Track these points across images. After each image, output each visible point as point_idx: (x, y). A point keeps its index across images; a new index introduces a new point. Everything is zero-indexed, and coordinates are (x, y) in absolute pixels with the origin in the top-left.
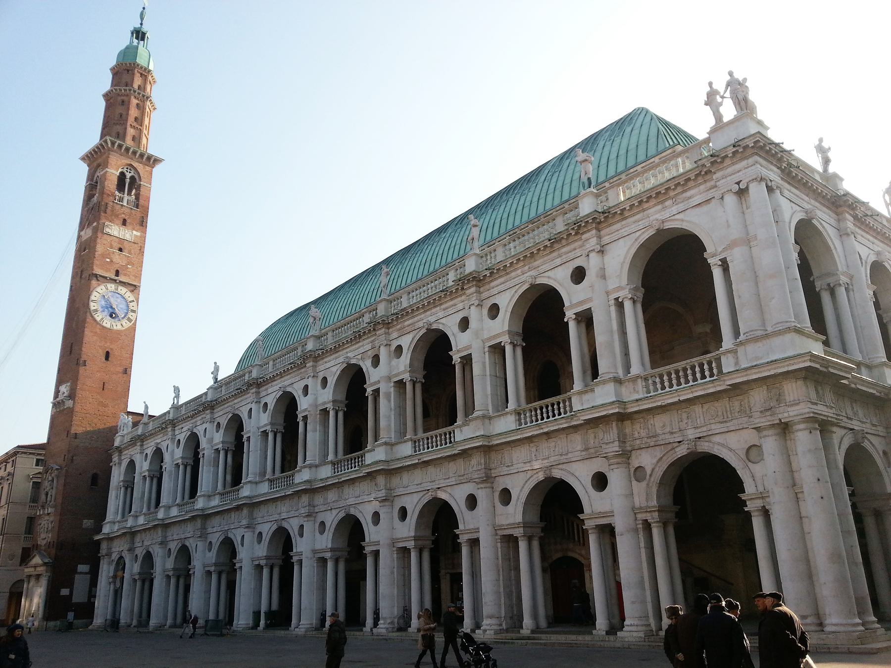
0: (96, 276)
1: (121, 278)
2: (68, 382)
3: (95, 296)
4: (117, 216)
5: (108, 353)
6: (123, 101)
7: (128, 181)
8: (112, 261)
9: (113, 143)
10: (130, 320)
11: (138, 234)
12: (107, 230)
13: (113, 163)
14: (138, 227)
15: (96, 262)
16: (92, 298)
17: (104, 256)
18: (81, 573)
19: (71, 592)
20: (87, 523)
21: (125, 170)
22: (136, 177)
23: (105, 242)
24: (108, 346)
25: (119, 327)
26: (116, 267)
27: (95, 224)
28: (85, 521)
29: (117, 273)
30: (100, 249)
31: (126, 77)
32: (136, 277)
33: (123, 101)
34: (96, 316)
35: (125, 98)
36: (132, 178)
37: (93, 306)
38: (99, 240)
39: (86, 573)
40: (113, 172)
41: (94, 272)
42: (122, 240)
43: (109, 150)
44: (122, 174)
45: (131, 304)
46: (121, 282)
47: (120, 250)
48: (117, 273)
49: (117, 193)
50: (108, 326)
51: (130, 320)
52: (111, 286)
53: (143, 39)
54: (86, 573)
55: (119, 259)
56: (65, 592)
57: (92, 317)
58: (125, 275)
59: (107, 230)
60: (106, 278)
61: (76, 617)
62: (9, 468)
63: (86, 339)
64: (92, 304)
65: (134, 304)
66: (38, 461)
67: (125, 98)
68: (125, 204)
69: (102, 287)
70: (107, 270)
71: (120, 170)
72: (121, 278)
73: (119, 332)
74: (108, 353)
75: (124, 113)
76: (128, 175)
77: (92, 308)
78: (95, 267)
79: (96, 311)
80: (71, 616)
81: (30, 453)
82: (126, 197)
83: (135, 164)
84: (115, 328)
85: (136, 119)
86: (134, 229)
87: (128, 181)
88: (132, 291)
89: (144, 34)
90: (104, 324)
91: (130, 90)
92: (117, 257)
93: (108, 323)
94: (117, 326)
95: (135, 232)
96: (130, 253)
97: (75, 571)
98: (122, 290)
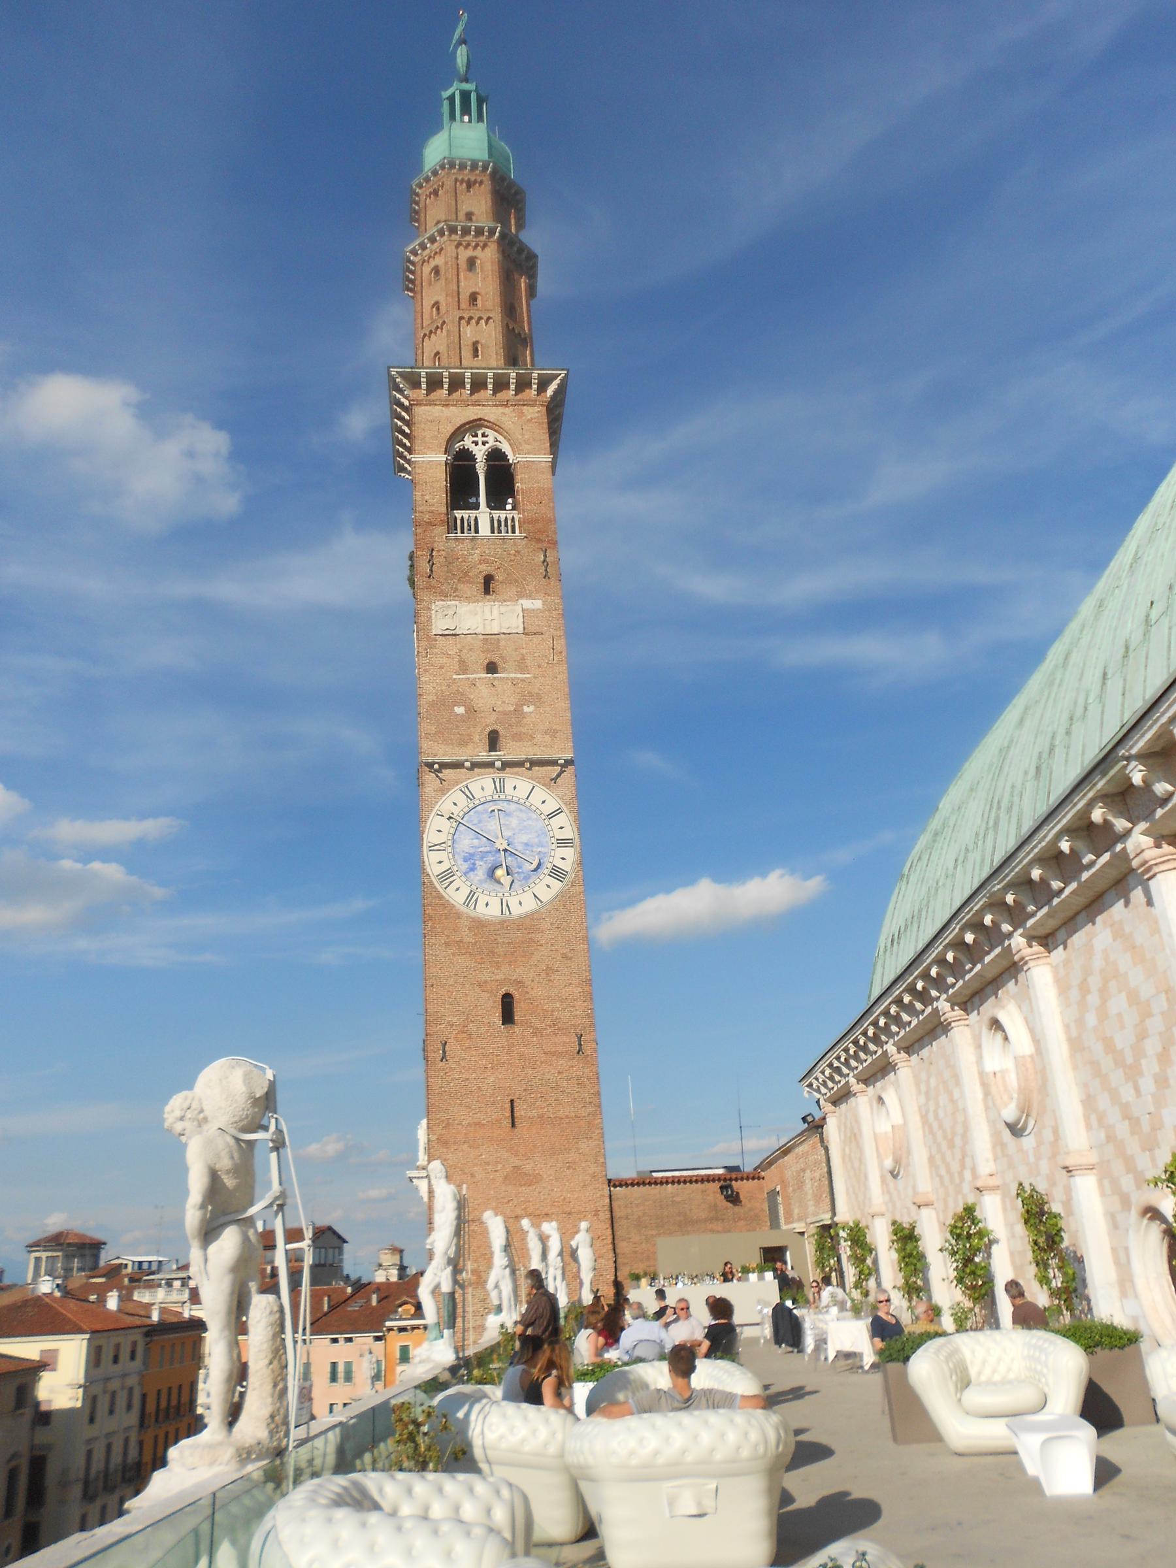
0: (430, 765)
3: (435, 830)
4: (465, 577)
6: (436, 271)
8: (472, 711)
10: (557, 873)
11: (538, 604)
12: (439, 625)
13: (428, 434)
15: (427, 727)
17: (443, 703)
21: (467, 442)
22: (505, 447)
24: (502, 976)
25: (530, 905)
26: (490, 722)
29: (494, 741)
30: (430, 687)
32: (553, 733)
33: (436, 271)
35: (439, 261)
36: (496, 456)
37: (435, 863)
41: (425, 759)
42: (490, 640)
46: (506, 765)
47: (492, 668)
49: (458, 514)
51: (557, 873)
52: (482, 785)
55: (491, 697)
57: (441, 897)
58: (518, 738)
59: (439, 625)
60: (457, 765)
68: (484, 529)
69: (456, 795)
70: (464, 741)
73: (531, 922)
75: (441, 299)
76: (480, 453)
78: (425, 745)
79: (447, 875)
82: (484, 515)
83: (490, 413)
84: (517, 911)
85: (473, 297)
86: (521, 595)
90: (481, 909)
92: (484, 690)
93: (489, 908)
94: (523, 904)
95: (527, 603)
96: (522, 666)
98: (518, 785)
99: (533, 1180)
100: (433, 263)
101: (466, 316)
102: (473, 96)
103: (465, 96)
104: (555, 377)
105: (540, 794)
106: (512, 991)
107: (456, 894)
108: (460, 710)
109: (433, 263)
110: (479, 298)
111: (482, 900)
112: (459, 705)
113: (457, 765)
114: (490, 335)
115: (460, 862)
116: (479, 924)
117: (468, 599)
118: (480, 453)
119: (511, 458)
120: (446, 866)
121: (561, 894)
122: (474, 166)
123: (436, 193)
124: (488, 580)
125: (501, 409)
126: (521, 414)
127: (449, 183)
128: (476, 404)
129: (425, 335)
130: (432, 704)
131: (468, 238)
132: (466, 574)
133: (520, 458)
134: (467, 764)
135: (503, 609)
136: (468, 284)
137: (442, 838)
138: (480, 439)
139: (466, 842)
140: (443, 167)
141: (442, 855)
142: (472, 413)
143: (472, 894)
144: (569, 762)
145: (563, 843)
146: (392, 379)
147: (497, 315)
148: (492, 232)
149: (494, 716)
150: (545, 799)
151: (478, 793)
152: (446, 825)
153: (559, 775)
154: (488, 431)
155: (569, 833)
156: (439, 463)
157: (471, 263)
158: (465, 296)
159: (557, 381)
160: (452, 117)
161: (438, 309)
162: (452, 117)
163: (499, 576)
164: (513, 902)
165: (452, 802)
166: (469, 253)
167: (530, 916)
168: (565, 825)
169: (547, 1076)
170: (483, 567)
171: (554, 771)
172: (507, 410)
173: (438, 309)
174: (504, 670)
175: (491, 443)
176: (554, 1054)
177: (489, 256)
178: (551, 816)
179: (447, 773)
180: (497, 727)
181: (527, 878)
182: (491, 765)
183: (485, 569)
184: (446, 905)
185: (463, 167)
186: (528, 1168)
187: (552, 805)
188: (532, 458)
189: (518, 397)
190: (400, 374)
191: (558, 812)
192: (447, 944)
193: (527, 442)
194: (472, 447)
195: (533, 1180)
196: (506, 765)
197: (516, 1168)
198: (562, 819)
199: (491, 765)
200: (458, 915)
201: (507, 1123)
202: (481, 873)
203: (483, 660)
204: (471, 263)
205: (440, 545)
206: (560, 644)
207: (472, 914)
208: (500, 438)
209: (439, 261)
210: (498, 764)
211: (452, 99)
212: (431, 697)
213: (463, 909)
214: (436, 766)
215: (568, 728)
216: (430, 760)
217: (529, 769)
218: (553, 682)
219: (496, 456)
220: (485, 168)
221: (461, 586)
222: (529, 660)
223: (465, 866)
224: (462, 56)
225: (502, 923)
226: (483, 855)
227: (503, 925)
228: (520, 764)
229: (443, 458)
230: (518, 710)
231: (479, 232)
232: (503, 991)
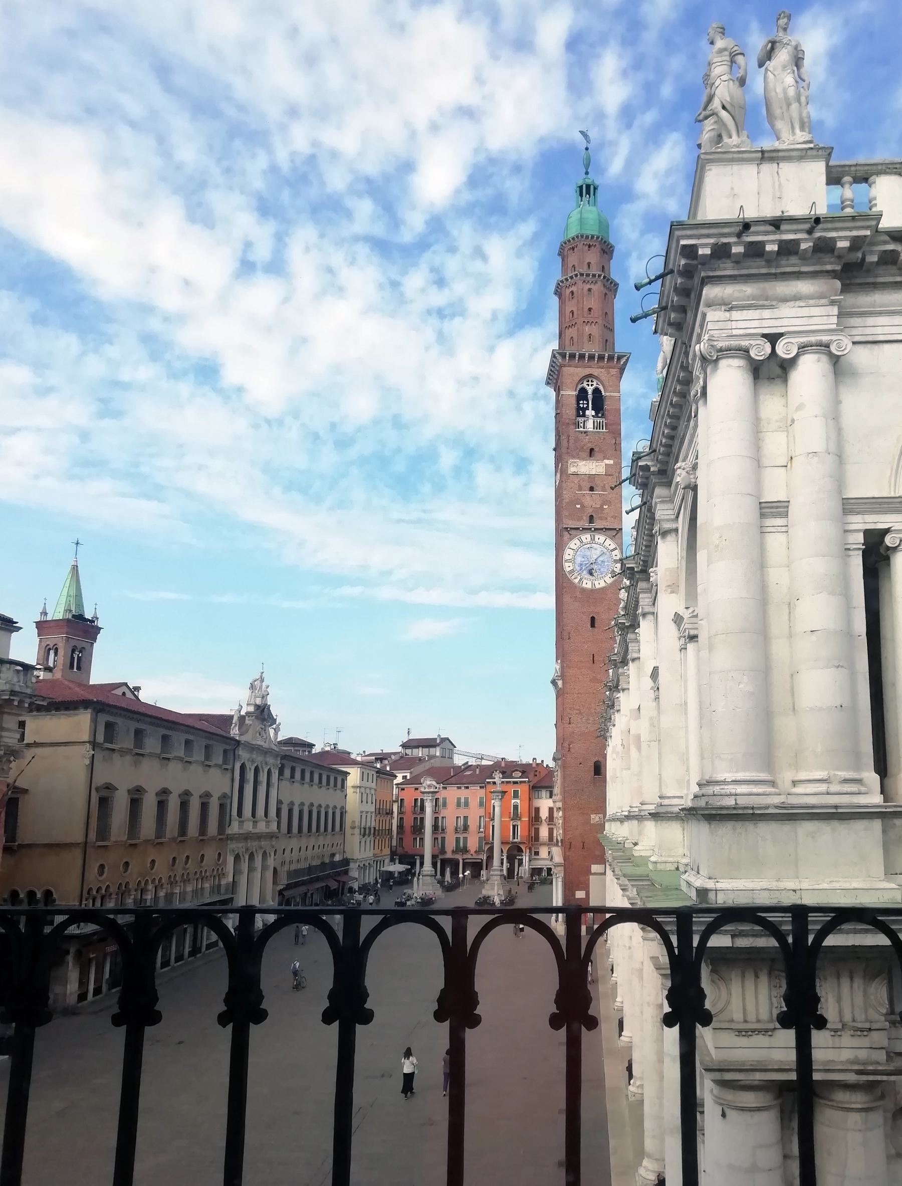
1: (598, 524)
3: (568, 554)
4: (582, 449)
5: (593, 619)
6: (572, 293)
7: (590, 397)
8: (583, 506)
9: (563, 356)
11: (611, 462)
16: (566, 557)
17: (573, 503)
18: (595, 874)
19: (588, 894)
22: (601, 388)
25: (603, 584)
26: (590, 511)
28: (593, 816)
29: (591, 519)
30: (567, 495)
31: (573, 259)
32: (615, 517)
33: (572, 293)
35: (573, 288)
36: (596, 391)
40: (571, 393)
42: (591, 477)
43: (561, 366)
45: (614, 553)
47: (592, 489)
48: (591, 517)
50: (589, 586)
52: (586, 537)
53: (588, 192)
55: (591, 501)
56: (580, 894)
58: (601, 518)
59: (572, 470)
65: (617, 552)
69: (576, 541)
71: (580, 386)
72: (598, 524)
74: (593, 619)
76: (590, 390)
77: (568, 569)
79: (572, 571)
83: (595, 372)
84: (598, 586)
85: (590, 309)
86: (605, 458)
87: (590, 397)
88: (613, 538)
90: (584, 585)
91: (576, 275)
92: (588, 498)
93: (587, 584)
95: (607, 462)
96: (604, 489)
97: (589, 872)
98: (600, 538)
100: (571, 289)
102: (592, 188)
103: (588, 186)
105: (608, 541)
108: (578, 506)
109: (571, 289)
114: (595, 330)
116: (584, 590)
117: (584, 459)
118: (590, 390)
120: (571, 568)
122: (593, 237)
123: (573, 249)
124: (592, 450)
126: (609, 373)
131: (588, 279)
133: (607, 394)
137: (570, 557)
138: (590, 383)
139: (579, 559)
140: (577, 237)
141: (570, 564)
142: (588, 371)
143: (581, 579)
147: (600, 321)
148: (599, 276)
149: (591, 510)
151: (584, 541)
152: (571, 552)
158: (586, 309)
160: (581, 195)
162: (581, 195)
163: (596, 449)
164: (596, 583)
165: (574, 544)
166: (588, 286)
167: (602, 589)
171: (614, 533)
177: (597, 288)
178: (612, 550)
179: (573, 532)
183: (590, 445)
185: (587, 237)
187: (613, 546)
188: (612, 394)
191: (615, 549)
200: (576, 587)
204: (590, 290)
205: (572, 434)
209: (573, 288)
211: (581, 187)
219: (596, 391)
227: (593, 591)
229: (575, 393)
230: (602, 507)
231: (594, 276)
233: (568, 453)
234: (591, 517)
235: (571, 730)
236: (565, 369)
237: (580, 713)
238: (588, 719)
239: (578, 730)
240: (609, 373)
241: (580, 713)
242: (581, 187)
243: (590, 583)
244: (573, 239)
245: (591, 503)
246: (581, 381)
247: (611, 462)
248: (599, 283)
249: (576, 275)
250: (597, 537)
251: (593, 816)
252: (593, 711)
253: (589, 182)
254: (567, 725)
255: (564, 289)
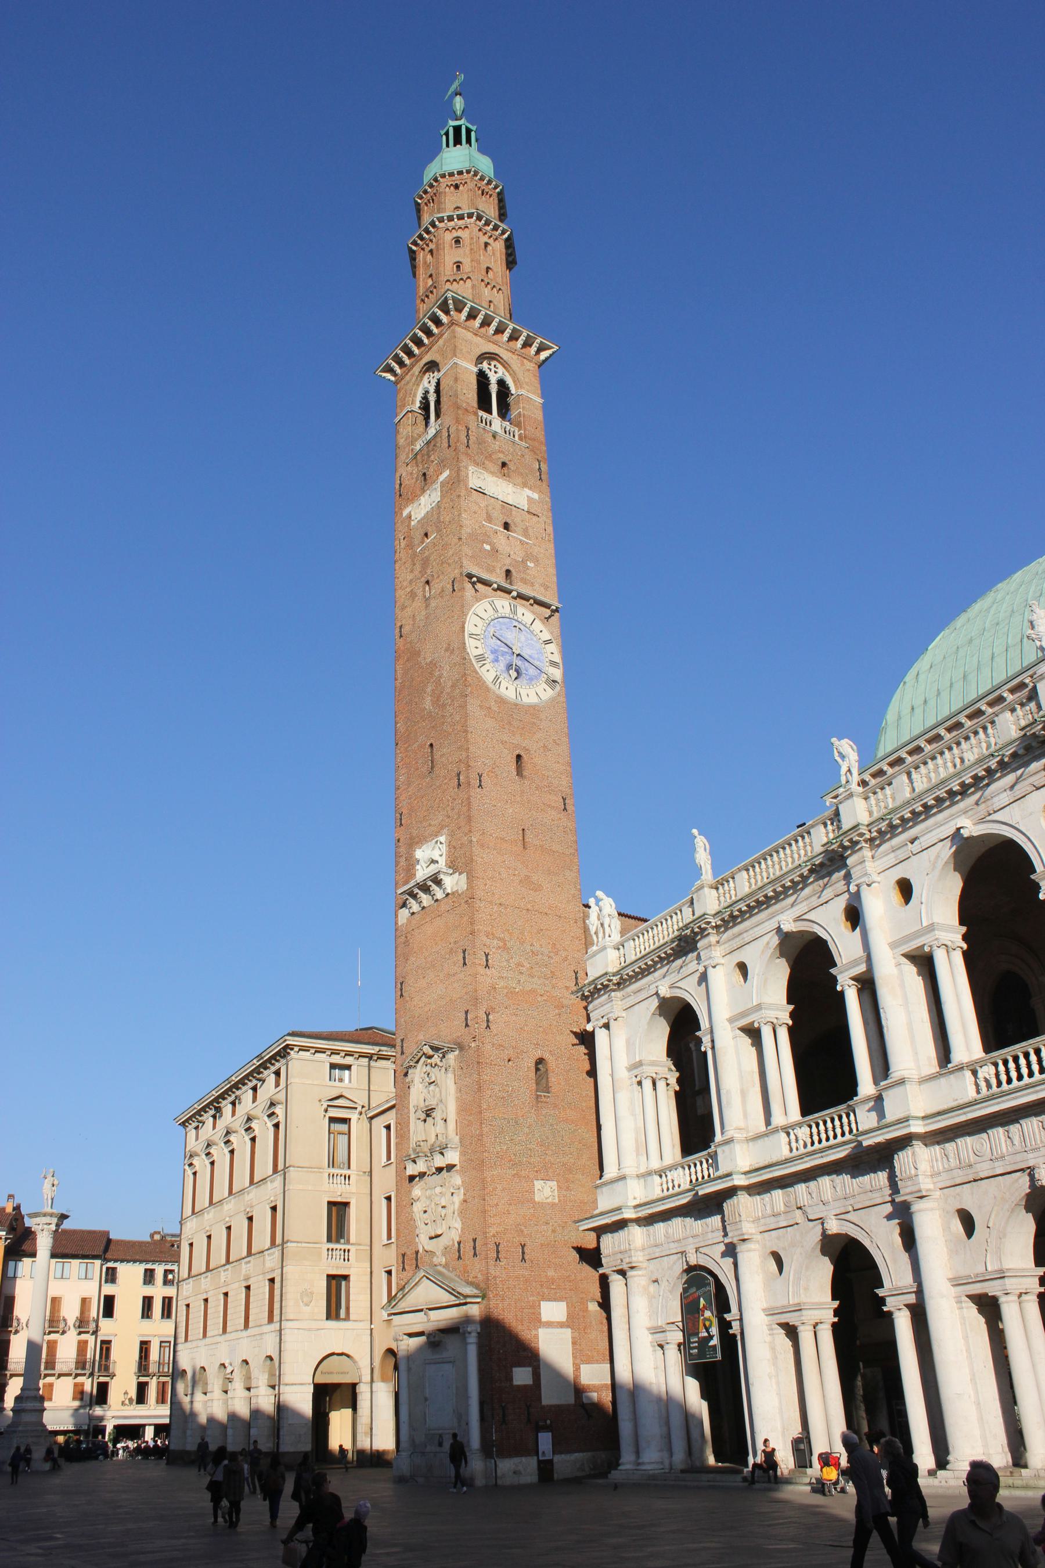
0: (470, 576)
2: (437, 834)
4: (489, 457)
5: (519, 757)
6: (457, 241)
7: (494, 389)
8: (495, 551)
11: (536, 496)
12: (474, 482)
14: (533, 480)
15: (467, 550)
16: (469, 628)
18: (549, 1324)
19: (536, 1376)
20: (545, 1191)
21: (485, 365)
23: (475, 508)
25: (533, 700)
26: (507, 563)
27: (446, 474)
28: (538, 1184)
30: (469, 523)
32: (546, 588)
33: (457, 241)
34: (482, 671)
35: (460, 233)
36: (501, 383)
38: (464, 504)
39: (561, 1325)
43: (452, 323)
44: (482, 379)
46: (521, 596)
47: (506, 526)
49: (481, 413)
52: (503, 604)
53: (469, 141)
54: (561, 1325)
55: (510, 547)
56: (522, 1376)
57: (477, 673)
58: (524, 581)
59: (474, 482)
60: (487, 583)
61: (558, 1446)
62: (268, 1089)
63: (471, 722)
64: (471, 644)
66: (333, 1066)
67: (460, 233)
70: (491, 570)
72: (519, 587)
76: (493, 379)
79: (481, 658)
80: (545, 1440)
81: (319, 1051)
84: (526, 700)
85: (488, 269)
86: (525, 485)
87: (494, 389)
89: (469, 131)
93: (508, 689)
95: (527, 492)
96: (526, 532)
97: (537, 1321)
98: (526, 614)
99: (538, 888)
100: (455, 234)
101: (486, 281)
102: (473, 134)
103: (469, 131)
104: (550, 348)
105: (538, 625)
106: (522, 754)
107: (488, 673)
108: (488, 547)
109: (455, 234)
110: (490, 272)
111: (504, 684)
112: (487, 543)
113: (487, 583)
115: (489, 652)
116: (501, 701)
117: (492, 473)
119: (513, 391)
121: (553, 700)
123: (457, 187)
125: (510, 354)
126: (523, 364)
127: (471, 185)
128: (495, 343)
129: (448, 281)
130: (470, 535)
132: (490, 455)
134: (495, 586)
135: (514, 490)
136: (485, 261)
138: (492, 367)
140: (468, 172)
141: (478, 644)
142: (491, 348)
143: (497, 678)
144: (557, 610)
145: (553, 664)
146: (446, 300)
149: (508, 561)
150: (543, 631)
153: (550, 617)
154: (498, 365)
155: (557, 658)
156: (472, 372)
157: (486, 244)
159: (550, 352)
161: (458, 267)
163: (511, 466)
164: (523, 692)
166: (485, 239)
167: (533, 707)
168: (553, 653)
169: (545, 820)
170: (501, 455)
171: (547, 612)
172: (515, 357)
173: (458, 267)
174: (515, 532)
175: (500, 375)
176: (549, 806)
178: (548, 642)
179: (479, 586)
180: (511, 569)
181: (531, 679)
182: (509, 592)
184: (480, 679)
186: (535, 878)
187: (546, 636)
188: (531, 396)
189: (523, 351)
190: (454, 298)
192: (481, 707)
193: (527, 384)
194: (488, 372)
195: (538, 888)
196: (521, 596)
197: (527, 877)
198: (552, 647)
199: (509, 592)
200: (488, 689)
201: (520, 844)
202: (502, 665)
203: (502, 519)
206: (550, 529)
207: (497, 692)
208: (506, 374)
210: (514, 594)
212: (469, 530)
213: (491, 686)
214: (474, 579)
215: (554, 587)
216: (474, 572)
217: (532, 605)
218: (546, 551)
219: (501, 383)
220: (496, 188)
221: (487, 462)
222: (530, 531)
223: (492, 657)
224: (459, 103)
225: (516, 705)
226: (504, 654)
228: (526, 598)
229: (475, 370)
232: (517, 752)
233: (467, 454)
234: (508, 573)
235: (489, 980)
236: (458, 329)
237: (505, 948)
238: (519, 964)
239: (502, 984)
240: (523, 364)
241: (505, 948)
242: (457, 130)
243: (512, 689)
244: (460, 173)
245: (508, 549)
246: (482, 358)
247: (536, 496)
248: (502, 243)
249: (470, 216)
250: (520, 610)
251: (538, 1184)
252: (528, 948)
253: (470, 126)
254: (482, 970)
255: (441, 232)
